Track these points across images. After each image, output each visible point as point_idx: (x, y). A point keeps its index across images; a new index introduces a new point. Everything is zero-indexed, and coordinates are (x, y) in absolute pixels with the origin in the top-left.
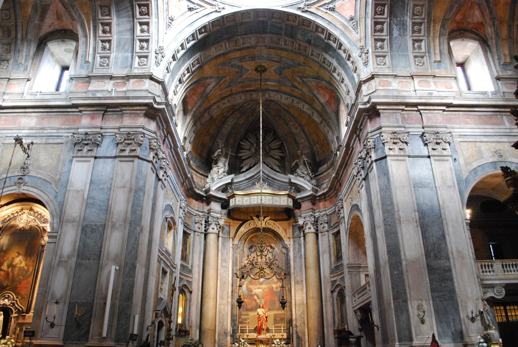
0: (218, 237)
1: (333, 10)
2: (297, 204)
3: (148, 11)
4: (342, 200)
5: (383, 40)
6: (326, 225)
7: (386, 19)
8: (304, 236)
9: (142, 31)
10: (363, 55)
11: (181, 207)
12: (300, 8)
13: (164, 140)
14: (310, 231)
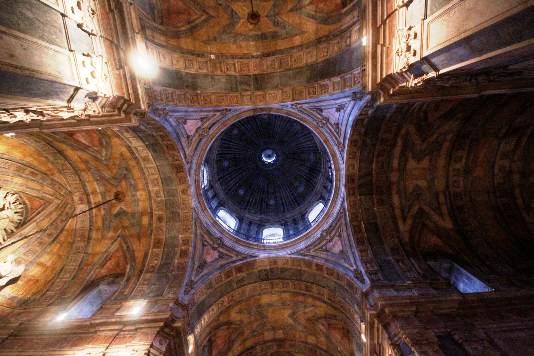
1: (204, 245)
12: (196, 220)
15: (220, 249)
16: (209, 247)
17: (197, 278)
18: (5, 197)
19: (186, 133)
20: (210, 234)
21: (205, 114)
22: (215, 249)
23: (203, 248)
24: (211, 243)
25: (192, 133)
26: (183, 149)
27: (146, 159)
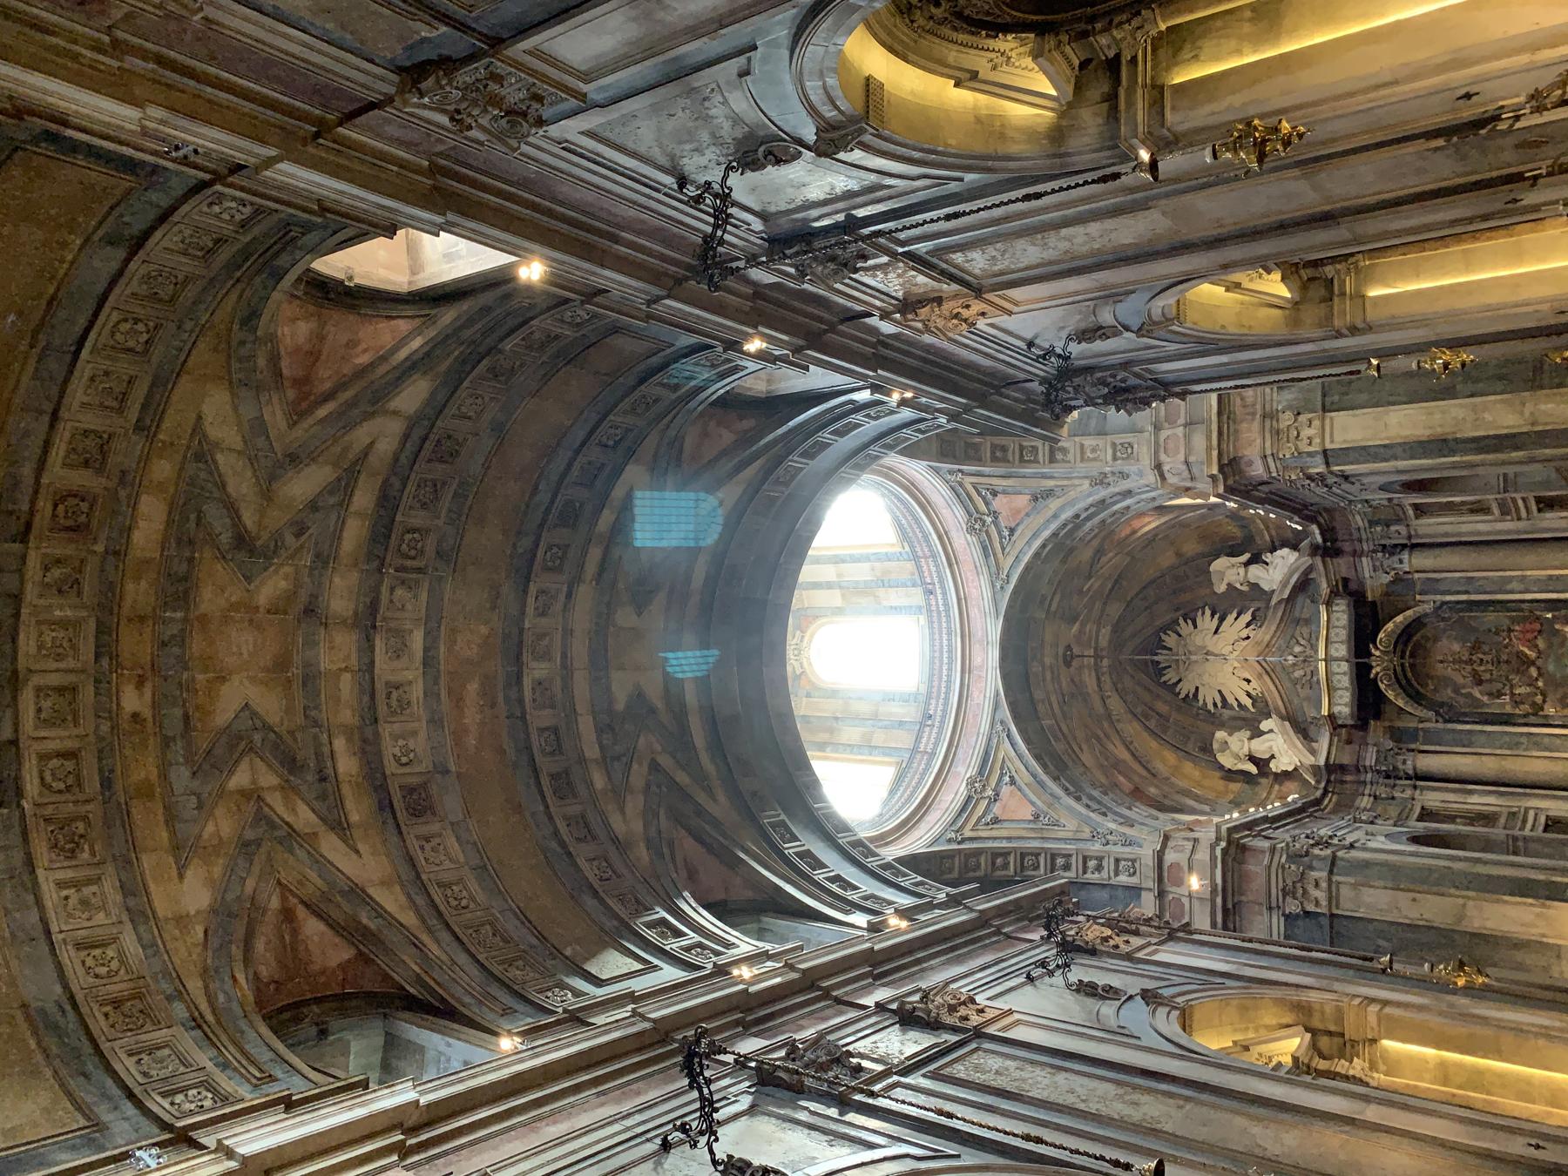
1: (1012, 531)
2: (1350, 590)
3: (1032, 854)
4: (1350, 501)
6: (1393, 528)
9: (1067, 867)
10: (1106, 481)
11: (1372, 823)
12: (1002, 588)
13: (1266, 838)
15: (983, 508)
17: (1076, 482)
18: (1180, 680)
20: (984, 548)
21: (994, 833)
22: (995, 512)
25: (1006, 790)
26: (1020, 757)
27: (1057, 739)
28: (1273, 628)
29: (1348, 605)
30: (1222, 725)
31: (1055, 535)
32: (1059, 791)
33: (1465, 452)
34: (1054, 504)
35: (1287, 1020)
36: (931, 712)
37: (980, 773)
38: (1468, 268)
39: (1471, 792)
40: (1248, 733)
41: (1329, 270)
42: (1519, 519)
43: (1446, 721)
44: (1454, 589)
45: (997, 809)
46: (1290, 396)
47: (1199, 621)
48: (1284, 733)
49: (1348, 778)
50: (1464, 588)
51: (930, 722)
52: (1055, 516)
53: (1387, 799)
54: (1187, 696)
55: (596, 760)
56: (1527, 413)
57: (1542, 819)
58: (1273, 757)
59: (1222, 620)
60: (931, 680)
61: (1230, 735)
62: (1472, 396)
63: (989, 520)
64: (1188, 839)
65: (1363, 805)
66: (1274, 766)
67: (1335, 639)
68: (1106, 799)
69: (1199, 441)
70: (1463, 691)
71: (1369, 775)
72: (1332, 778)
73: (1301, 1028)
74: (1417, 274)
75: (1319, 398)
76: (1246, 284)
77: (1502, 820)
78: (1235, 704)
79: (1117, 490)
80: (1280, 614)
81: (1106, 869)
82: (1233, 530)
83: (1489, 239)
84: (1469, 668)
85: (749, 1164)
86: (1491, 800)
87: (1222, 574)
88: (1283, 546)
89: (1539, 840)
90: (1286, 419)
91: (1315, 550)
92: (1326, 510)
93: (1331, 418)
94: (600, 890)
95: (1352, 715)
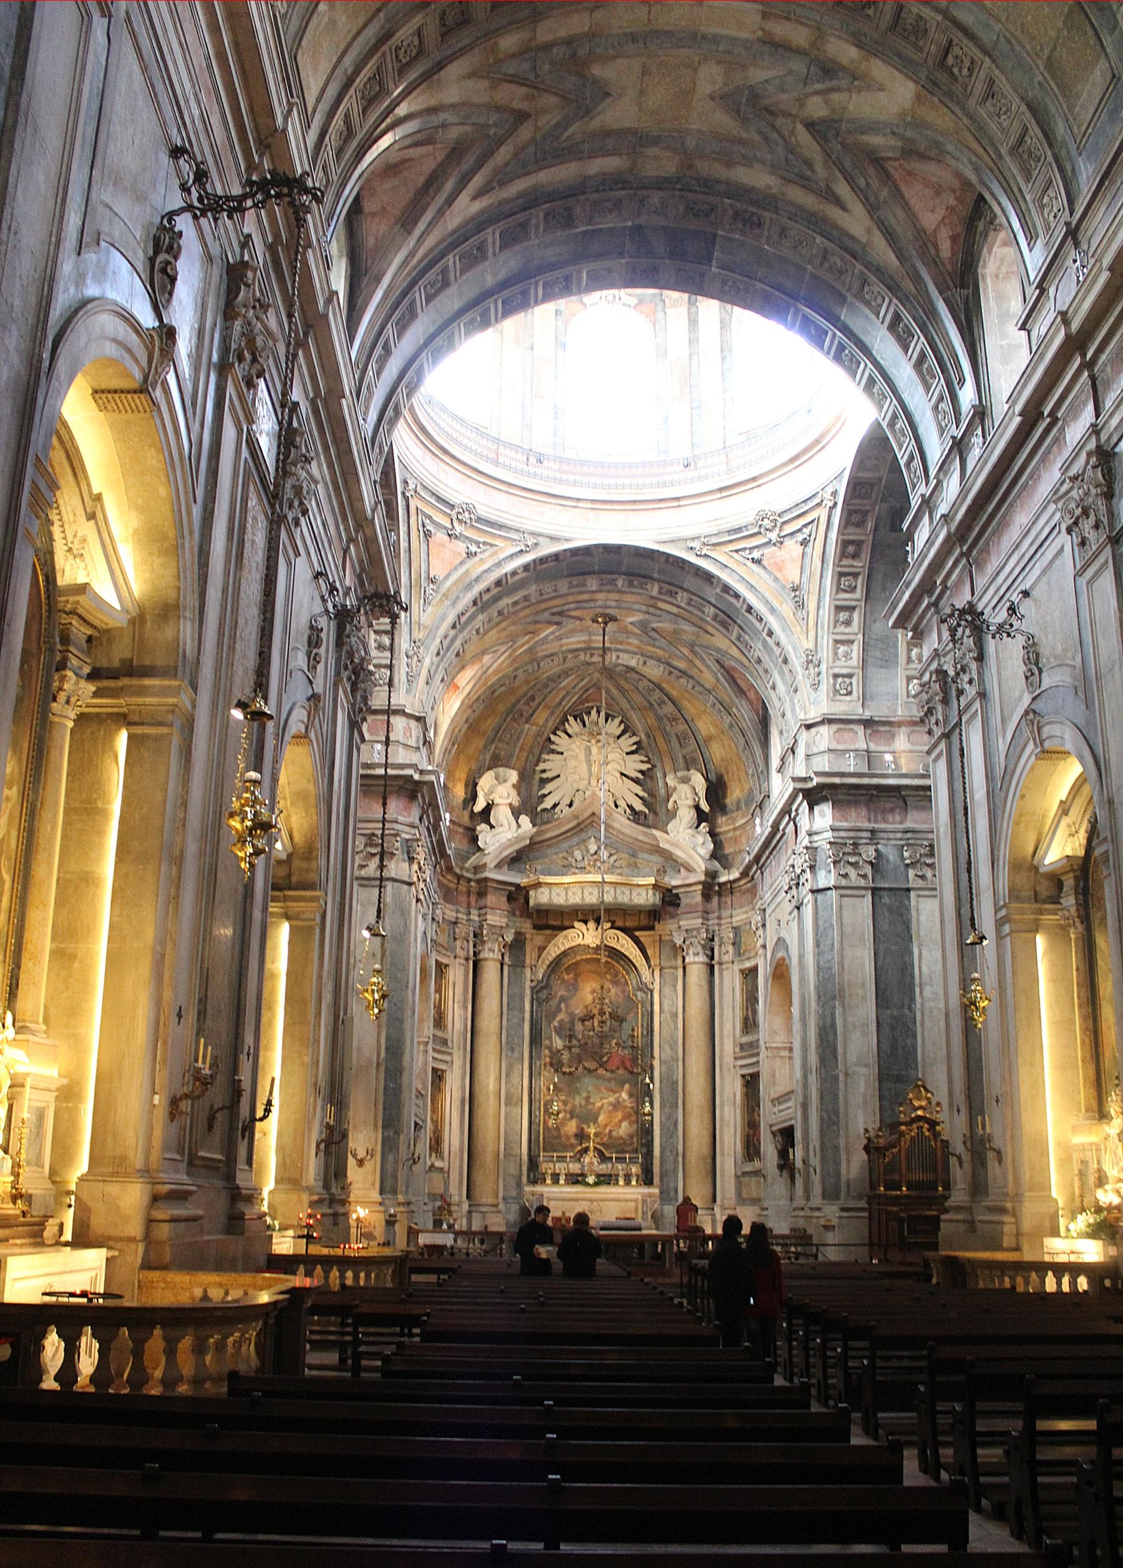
0: (502, 965)
1: (757, 562)
5: (852, 642)
6: (731, 948)
7: (858, 600)
8: (684, 968)
10: (811, 666)
11: (433, 919)
14: (697, 959)
15: (788, 529)
16: (767, 551)
17: (812, 634)
18: (570, 736)
19: (462, 563)
20: (739, 530)
21: (414, 533)
22: (782, 543)
23: (765, 568)
24: (761, 540)
25: (461, 547)
26: (498, 564)
28: (627, 832)
29: (654, 905)
30: (522, 776)
31: (750, 609)
32: (460, 607)
33: (822, 1017)
34: (786, 608)
35: (297, 837)
36: (545, 463)
37: (479, 520)
38: (1055, 1024)
39: (466, 1007)
40: (516, 804)
41: (1069, 901)
42: (736, 1059)
43: (532, 988)
44: (666, 1002)
45: (440, 537)
46: (891, 858)
47: (636, 757)
48: (518, 839)
49: (473, 899)
50: (666, 1008)
51: (532, 460)
52: (772, 610)
53: (454, 933)
54: (553, 743)
55: (535, 37)
56: (858, 1069)
57: (443, 1067)
58: (492, 827)
59: (636, 781)
60: (582, 463)
61: (514, 786)
62: (878, 1022)
63: (773, 536)
64: (418, 741)
65: (447, 911)
66: (482, 827)
67: (618, 892)
68: (451, 655)
69: (851, 764)
70: (563, 1005)
71: (476, 918)
72: (472, 884)
73: (290, 850)
74: (1053, 980)
75: (887, 886)
76: (1065, 821)
77: (439, 1033)
78: (545, 791)
79: (800, 677)
80: (641, 838)
81: (381, 655)
82: (734, 794)
83: (1083, 1043)
84: (596, 1011)
85: (176, 258)
86: (458, 1025)
87: (685, 780)
88: (715, 843)
89: (425, 1064)
90: (869, 852)
91: (712, 875)
92: (755, 886)
93: (863, 896)
94: (385, 48)
95: (539, 905)
